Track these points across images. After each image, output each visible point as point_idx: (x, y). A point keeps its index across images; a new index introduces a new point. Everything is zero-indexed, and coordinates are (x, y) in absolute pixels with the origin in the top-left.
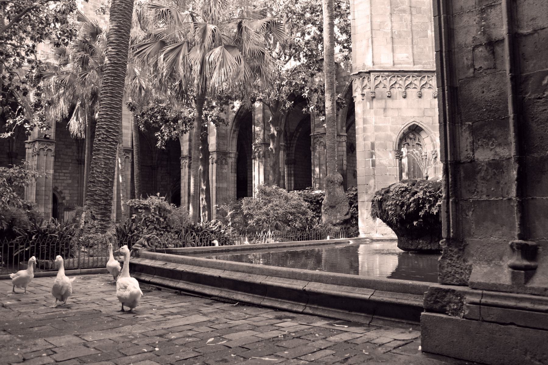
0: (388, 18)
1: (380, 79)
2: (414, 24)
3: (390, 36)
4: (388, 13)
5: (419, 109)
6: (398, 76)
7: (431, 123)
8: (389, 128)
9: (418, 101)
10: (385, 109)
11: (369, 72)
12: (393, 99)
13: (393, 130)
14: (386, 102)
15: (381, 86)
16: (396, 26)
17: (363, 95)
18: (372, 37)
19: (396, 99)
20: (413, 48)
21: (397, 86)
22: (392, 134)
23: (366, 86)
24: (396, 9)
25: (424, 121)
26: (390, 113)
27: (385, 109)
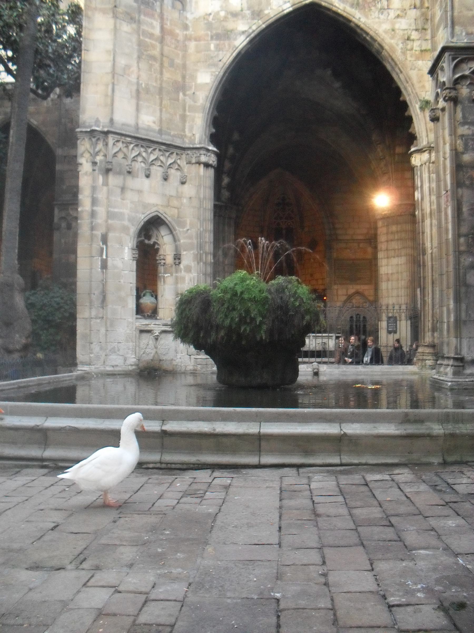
0: (134, 63)
1: (120, 145)
2: (165, 79)
3: (134, 88)
4: (135, 56)
5: (164, 195)
6: (142, 146)
7: (176, 216)
8: (126, 217)
9: (163, 185)
10: (123, 189)
11: (106, 133)
12: (133, 177)
13: (131, 220)
14: (124, 179)
15: (120, 155)
16: (144, 76)
17: (94, 163)
18: (113, 84)
19: (137, 177)
20: (161, 111)
21: (140, 159)
23: (99, 151)
24: (145, 53)
26: (129, 195)
27: (123, 189)
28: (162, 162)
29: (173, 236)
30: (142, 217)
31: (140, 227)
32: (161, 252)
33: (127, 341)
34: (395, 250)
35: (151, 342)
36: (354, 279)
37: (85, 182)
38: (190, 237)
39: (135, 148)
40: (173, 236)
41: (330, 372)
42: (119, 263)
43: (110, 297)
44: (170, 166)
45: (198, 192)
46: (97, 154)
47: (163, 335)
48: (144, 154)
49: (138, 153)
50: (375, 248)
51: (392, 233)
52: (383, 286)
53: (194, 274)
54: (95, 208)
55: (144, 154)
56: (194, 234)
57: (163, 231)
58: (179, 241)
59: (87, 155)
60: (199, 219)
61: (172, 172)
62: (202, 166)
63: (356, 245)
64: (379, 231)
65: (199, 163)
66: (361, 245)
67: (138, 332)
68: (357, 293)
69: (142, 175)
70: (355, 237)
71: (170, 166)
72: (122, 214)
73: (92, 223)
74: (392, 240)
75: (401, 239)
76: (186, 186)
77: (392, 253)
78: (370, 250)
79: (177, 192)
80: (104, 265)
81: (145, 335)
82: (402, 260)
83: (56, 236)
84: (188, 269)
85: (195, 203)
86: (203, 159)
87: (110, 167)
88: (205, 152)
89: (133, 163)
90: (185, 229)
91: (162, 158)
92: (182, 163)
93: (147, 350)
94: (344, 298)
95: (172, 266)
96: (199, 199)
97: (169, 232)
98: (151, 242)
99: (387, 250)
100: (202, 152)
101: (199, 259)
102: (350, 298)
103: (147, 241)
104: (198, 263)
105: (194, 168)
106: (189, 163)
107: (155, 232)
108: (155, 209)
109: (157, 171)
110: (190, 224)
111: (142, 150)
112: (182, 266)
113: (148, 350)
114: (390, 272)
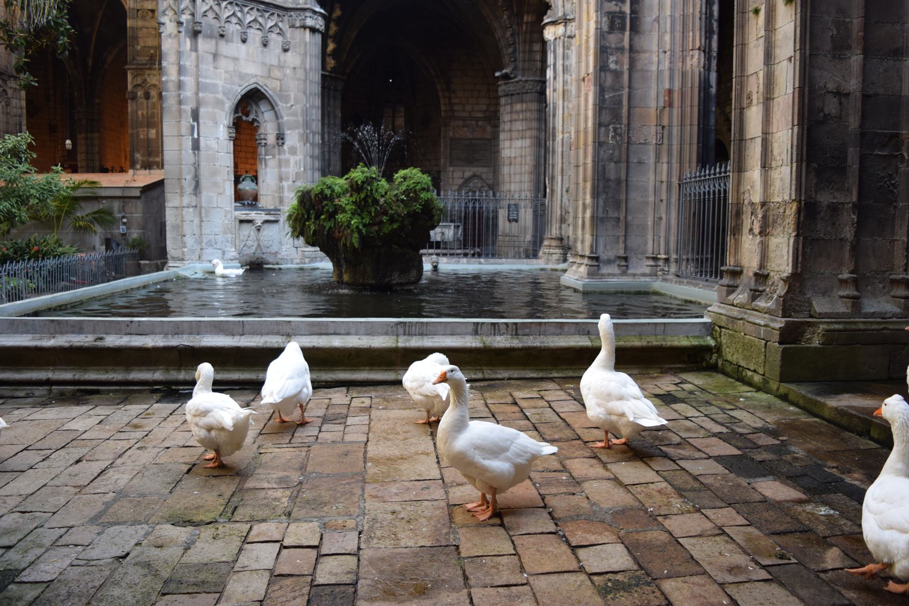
5: (264, 64)
8: (220, 89)
9: (262, 51)
10: (215, 56)
12: (227, 41)
15: (211, 15)
17: (180, 23)
19: (232, 42)
22: (225, 99)
25: (269, 85)
26: (222, 62)
27: (215, 56)
28: (260, 24)
29: (275, 112)
30: (239, 90)
31: (236, 101)
32: (262, 130)
33: (225, 233)
34: (519, 131)
35: (252, 233)
36: (470, 161)
37: (168, 46)
38: (294, 114)
39: (229, 6)
40: (275, 112)
41: (450, 266)
42: (213, 144)
43: (204, 182)
44: (270, 30)
45: (303, 62)
46: (183, 12)
47: (266, 226)
48: (239, 14)
49: (231, 12)
50: (496, 126)
51: (516, 112)
52: (505, 170)
53: (299, 157)
54: (182, 78)
55: (239, 14)
56: (299, 110)
57: (263, 107)
58: (282, 118)
59: (170, 13)
60: (305, 93)
61: (273, 36)
62: (308, 31)
63: (473, 122)
64: (502, 109)
65: (304, 27)
66: (480, 123)
67: (238, 222)
68: (474, 176)
69: (237, 38)
70: (474, 115)
71: (270, 30)
72: (215, 85)
73: (179, 95)
74: (516, 120)
75: (526, 120)
76: (289, 54)
77: (515, 135)
78: (489, 129)
79: (279, 61)
80: (196, 146)
81: (245, 226)
82: (527, 142)
83: (131, 107)
84: (293, 151)
85: (300, 74)
86: (310, 22)
87: (199, 28)
88: (311, 14)
89: (227, 25)
90: (289, 105)
91: (260, 19)
92: (284, 26)
93: (248, 243)
94: (461, 181)
95: (274, 147)
96: (305, 70)
97: (270, 108)
98: (250, 119)
99: (510, 131)
100: (308, 14)
101: (305, 139)
102: (467, 181)
103: (244, 118)
104: (304, 144)
105: (298, 33)
106: (292, 26)
107: (254, 107)
108: (253, 80)
109: (255, 35)
110: (295, 99)
111: (237, 9)
112: (285, 147)
113: (249, 243)
114: (513, 155)
